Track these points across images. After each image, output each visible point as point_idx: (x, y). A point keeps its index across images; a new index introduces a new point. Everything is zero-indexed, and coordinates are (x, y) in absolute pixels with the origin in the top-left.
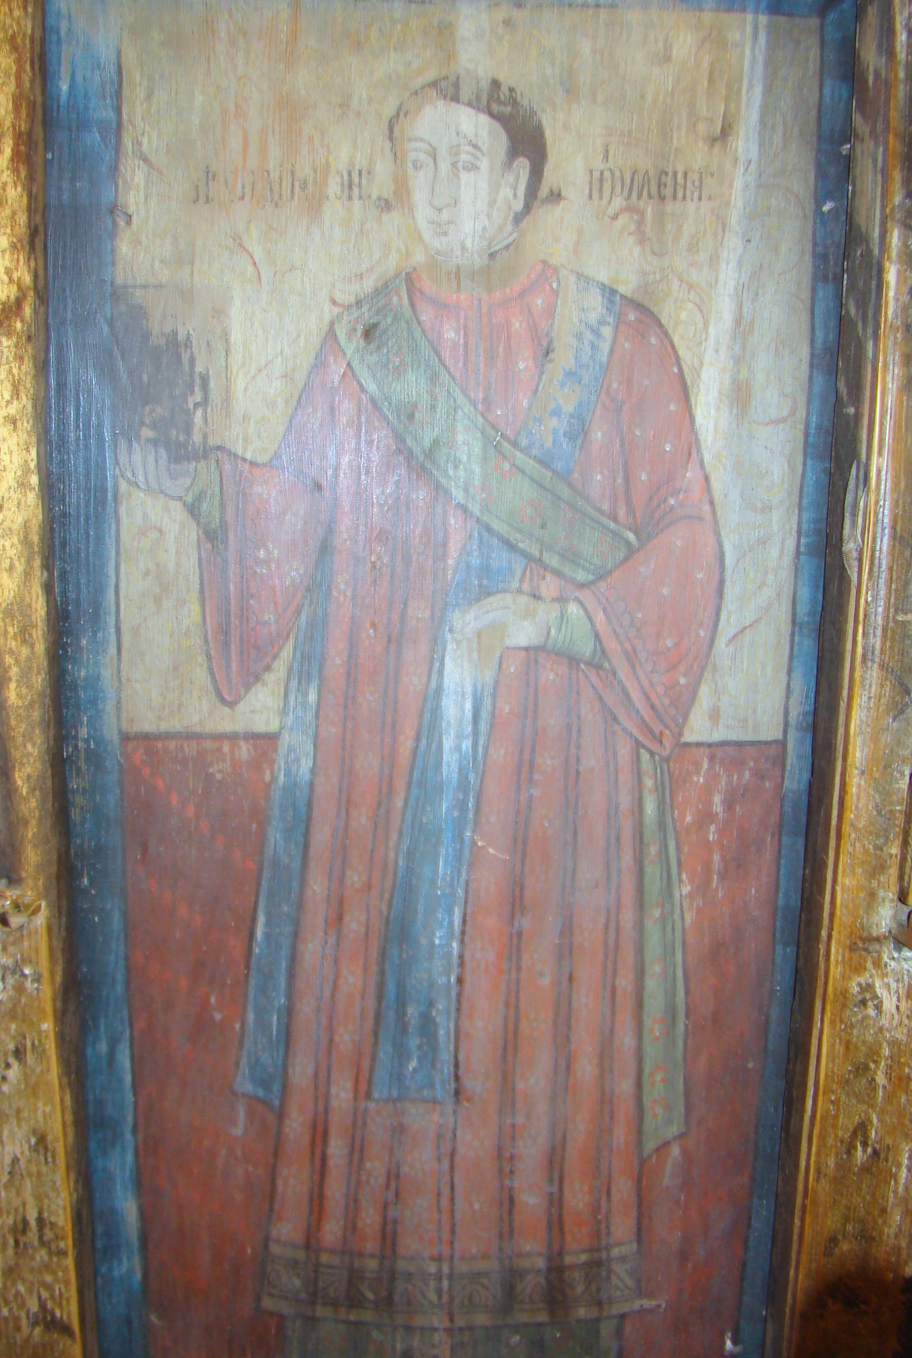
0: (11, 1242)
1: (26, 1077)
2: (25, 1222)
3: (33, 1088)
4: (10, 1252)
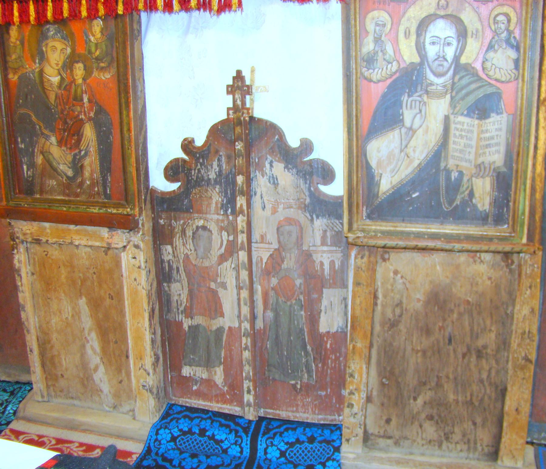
0: (520, 337)
1: (531, 293)
2: (525, 332)
3: (532, 296)
4: (520, 340)
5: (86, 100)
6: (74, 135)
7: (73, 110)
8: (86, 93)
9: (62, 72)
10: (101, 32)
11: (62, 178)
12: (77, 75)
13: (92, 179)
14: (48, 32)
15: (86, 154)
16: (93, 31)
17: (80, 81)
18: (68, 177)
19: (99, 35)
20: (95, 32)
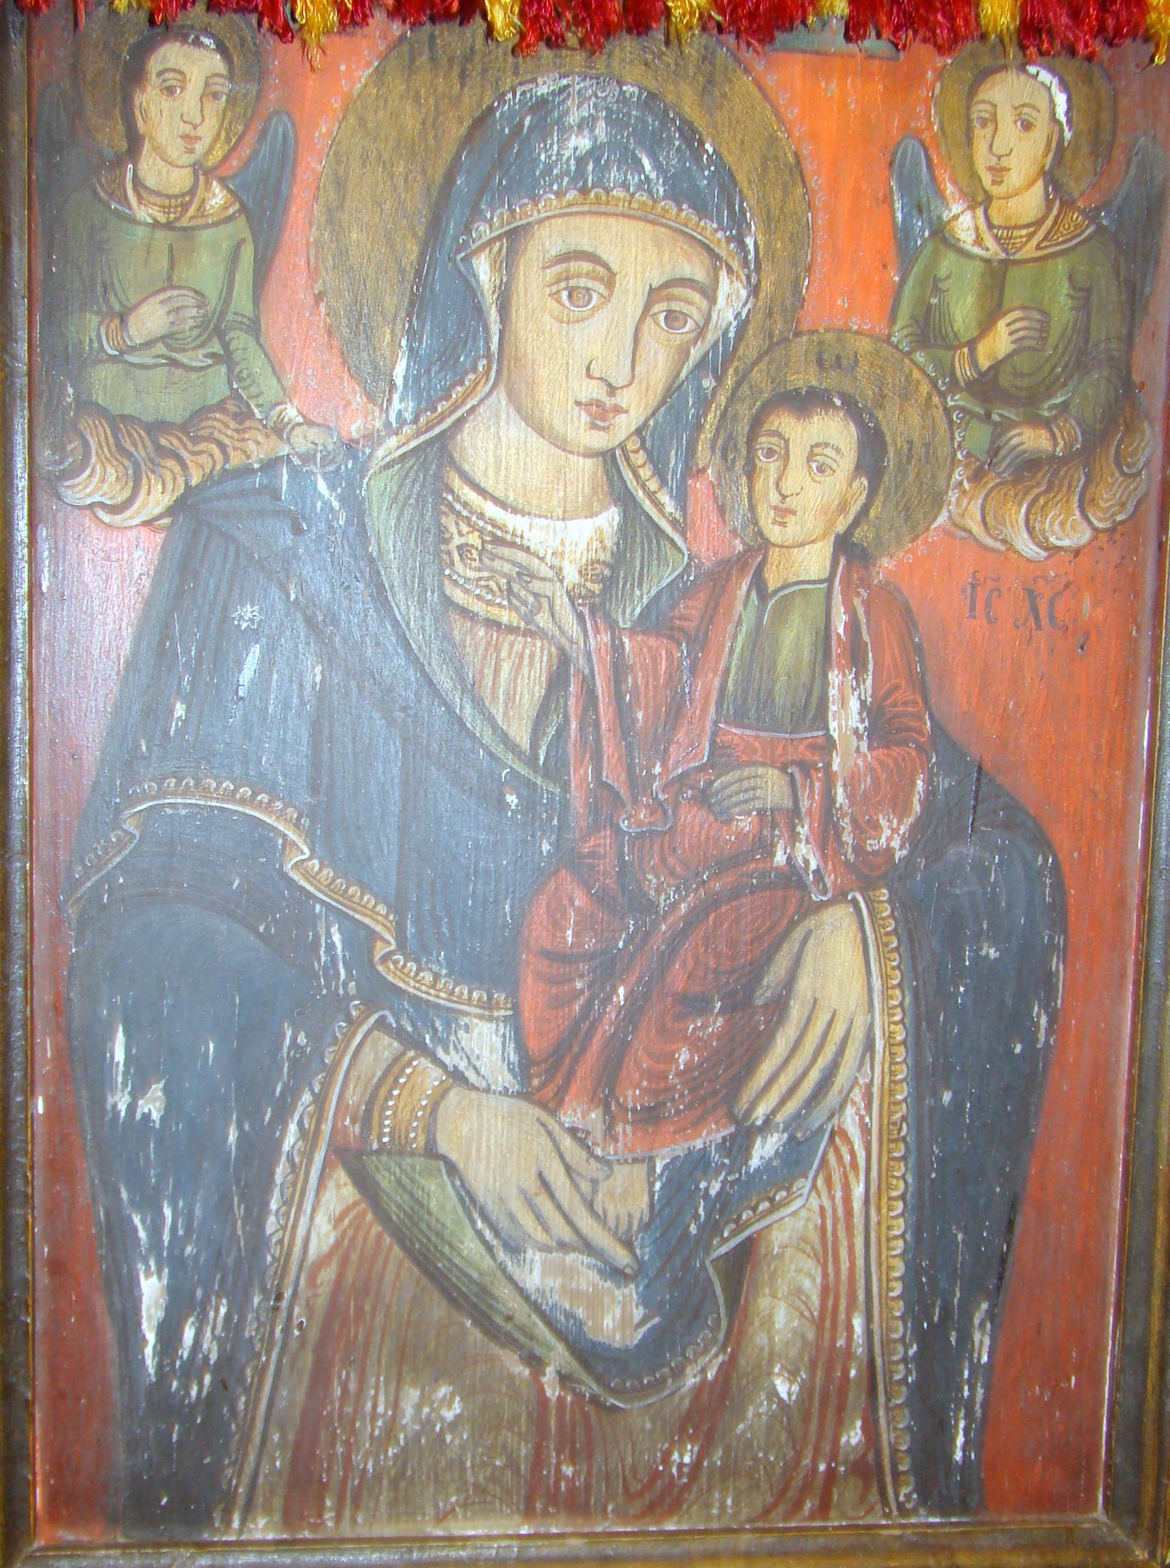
5: (846, 716)
6: (696, 1005)
7: (704, 798)
8: (856, 658)
9: (641, 478)
10: (1052, 178)
11: (535, 1363)
12: (783, 513)
13: (823, 1358)
14: (542, 130)
15: (795, 1159)
16: (982, 159)
17: (814, 561)
18: (588, 1354)
19: (1029, 203)
20: (999, 172)
